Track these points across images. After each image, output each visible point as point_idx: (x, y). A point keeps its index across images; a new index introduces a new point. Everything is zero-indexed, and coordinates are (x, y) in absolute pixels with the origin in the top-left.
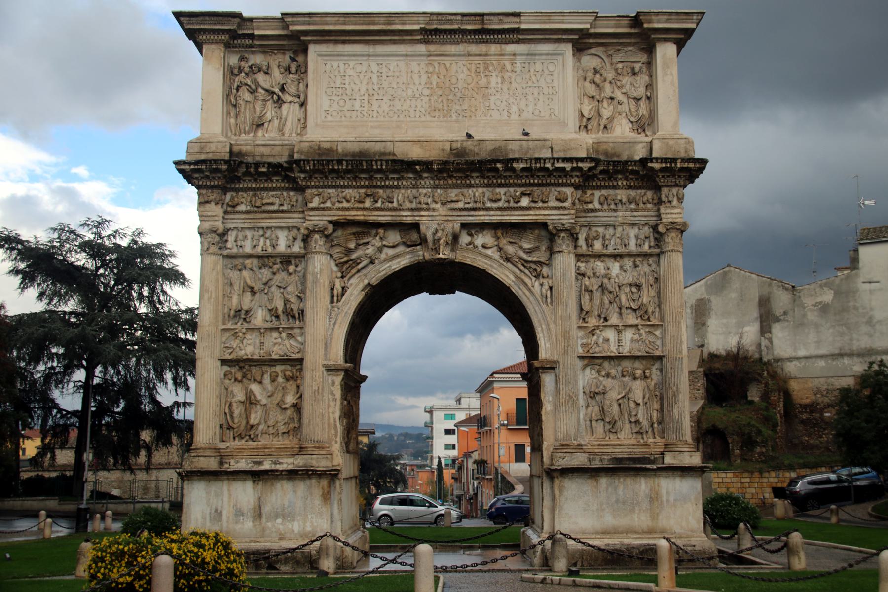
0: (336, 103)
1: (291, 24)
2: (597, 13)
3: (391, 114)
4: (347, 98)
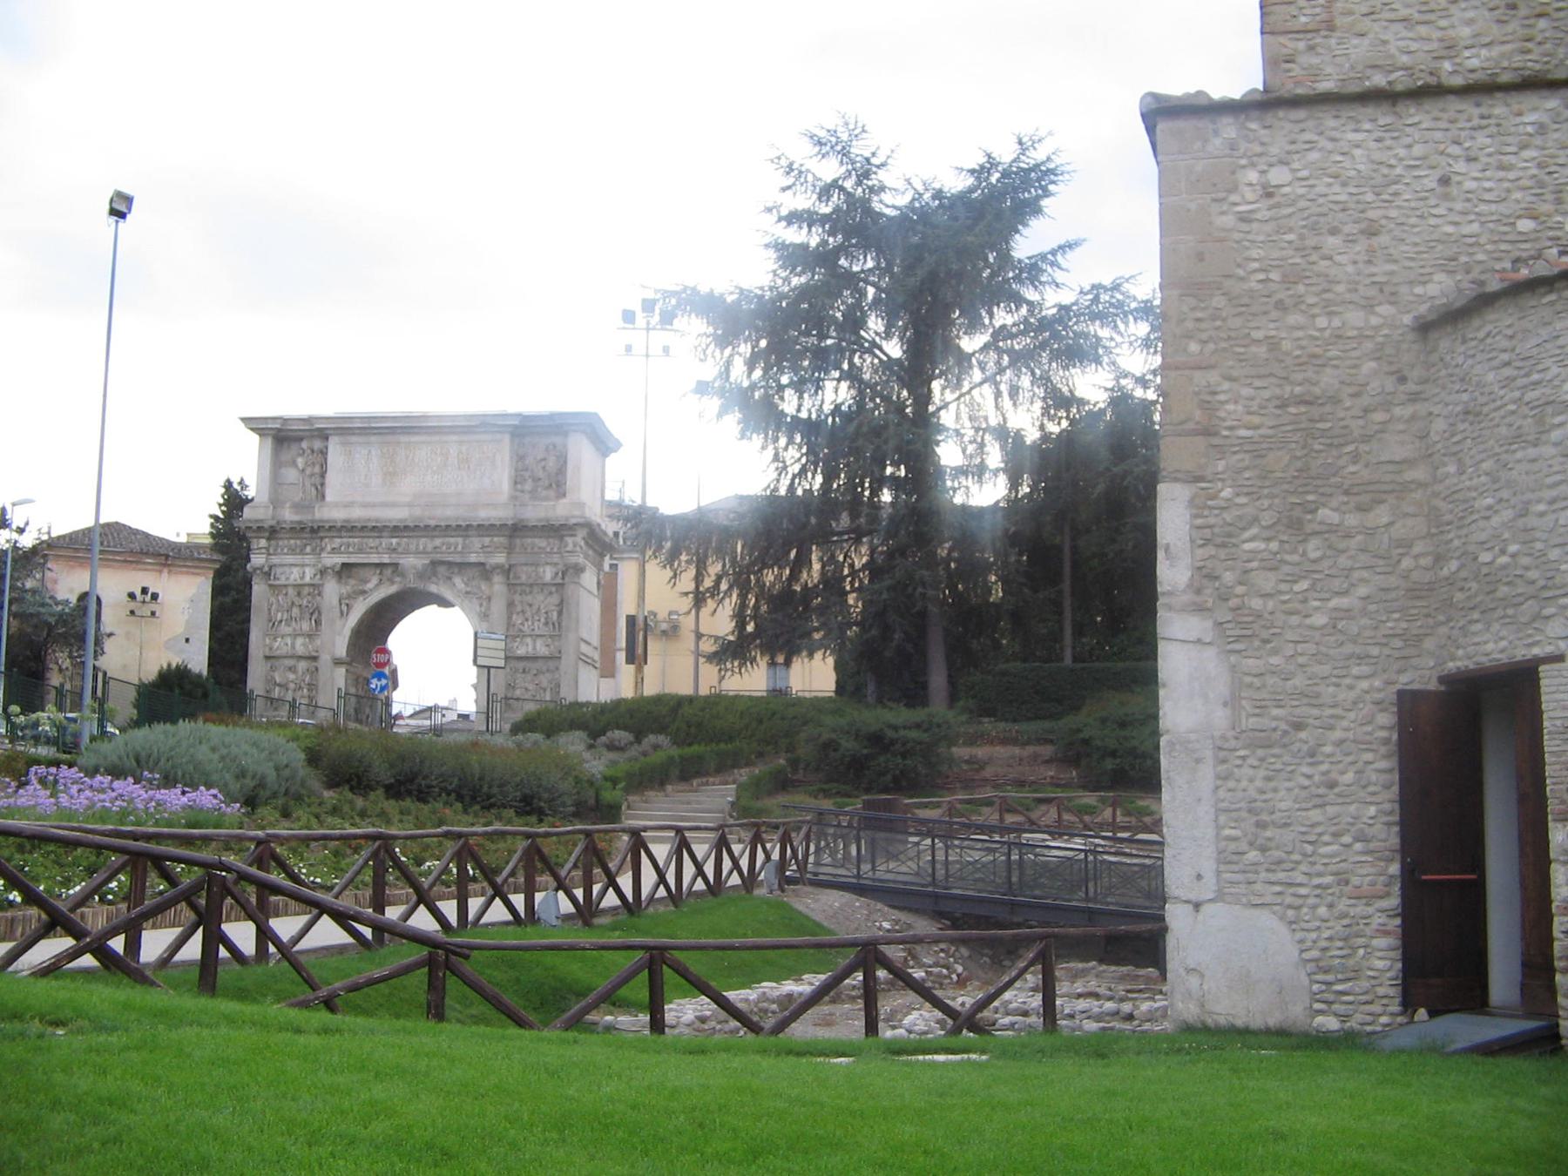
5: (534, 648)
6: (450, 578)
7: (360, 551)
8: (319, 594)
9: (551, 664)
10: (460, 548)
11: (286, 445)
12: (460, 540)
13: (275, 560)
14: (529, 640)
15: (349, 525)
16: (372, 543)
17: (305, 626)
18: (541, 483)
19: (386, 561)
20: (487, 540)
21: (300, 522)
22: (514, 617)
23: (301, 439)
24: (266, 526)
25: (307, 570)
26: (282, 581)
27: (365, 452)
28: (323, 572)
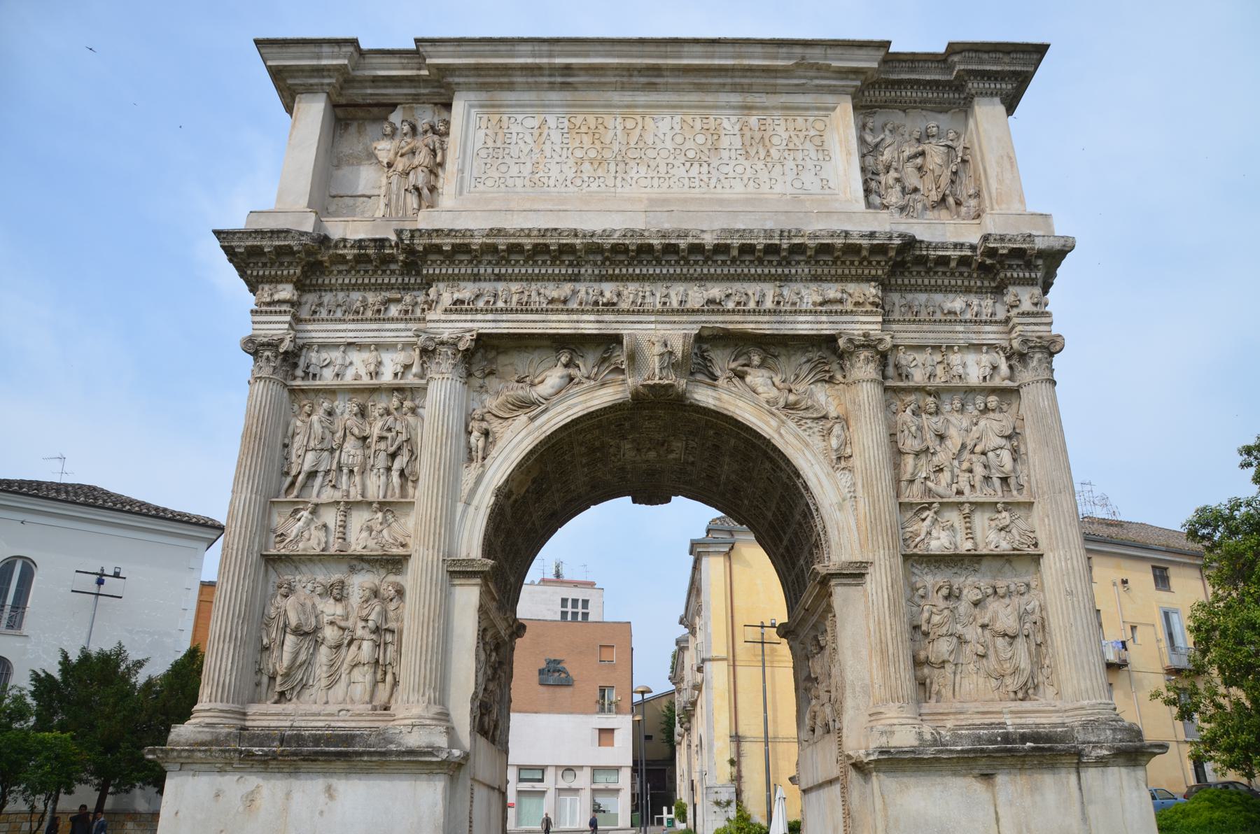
0: (494, 168)
1: (430, 57)
2: (887, 44)
3: (578, 182)
5: (970, 536)
6: (741, 376)
7: (524, 308)
8: (413, 411)
10: (769, 304)
11: (353, 129)
14: (954, 517)
15: (502, 243)
16: (552, 291)
18: (917, 196)
20: (832, 291)
21: (381, 243)
22: (909, 461)
23: (393, 106)
26: (327, 378)
27: (535, 123)
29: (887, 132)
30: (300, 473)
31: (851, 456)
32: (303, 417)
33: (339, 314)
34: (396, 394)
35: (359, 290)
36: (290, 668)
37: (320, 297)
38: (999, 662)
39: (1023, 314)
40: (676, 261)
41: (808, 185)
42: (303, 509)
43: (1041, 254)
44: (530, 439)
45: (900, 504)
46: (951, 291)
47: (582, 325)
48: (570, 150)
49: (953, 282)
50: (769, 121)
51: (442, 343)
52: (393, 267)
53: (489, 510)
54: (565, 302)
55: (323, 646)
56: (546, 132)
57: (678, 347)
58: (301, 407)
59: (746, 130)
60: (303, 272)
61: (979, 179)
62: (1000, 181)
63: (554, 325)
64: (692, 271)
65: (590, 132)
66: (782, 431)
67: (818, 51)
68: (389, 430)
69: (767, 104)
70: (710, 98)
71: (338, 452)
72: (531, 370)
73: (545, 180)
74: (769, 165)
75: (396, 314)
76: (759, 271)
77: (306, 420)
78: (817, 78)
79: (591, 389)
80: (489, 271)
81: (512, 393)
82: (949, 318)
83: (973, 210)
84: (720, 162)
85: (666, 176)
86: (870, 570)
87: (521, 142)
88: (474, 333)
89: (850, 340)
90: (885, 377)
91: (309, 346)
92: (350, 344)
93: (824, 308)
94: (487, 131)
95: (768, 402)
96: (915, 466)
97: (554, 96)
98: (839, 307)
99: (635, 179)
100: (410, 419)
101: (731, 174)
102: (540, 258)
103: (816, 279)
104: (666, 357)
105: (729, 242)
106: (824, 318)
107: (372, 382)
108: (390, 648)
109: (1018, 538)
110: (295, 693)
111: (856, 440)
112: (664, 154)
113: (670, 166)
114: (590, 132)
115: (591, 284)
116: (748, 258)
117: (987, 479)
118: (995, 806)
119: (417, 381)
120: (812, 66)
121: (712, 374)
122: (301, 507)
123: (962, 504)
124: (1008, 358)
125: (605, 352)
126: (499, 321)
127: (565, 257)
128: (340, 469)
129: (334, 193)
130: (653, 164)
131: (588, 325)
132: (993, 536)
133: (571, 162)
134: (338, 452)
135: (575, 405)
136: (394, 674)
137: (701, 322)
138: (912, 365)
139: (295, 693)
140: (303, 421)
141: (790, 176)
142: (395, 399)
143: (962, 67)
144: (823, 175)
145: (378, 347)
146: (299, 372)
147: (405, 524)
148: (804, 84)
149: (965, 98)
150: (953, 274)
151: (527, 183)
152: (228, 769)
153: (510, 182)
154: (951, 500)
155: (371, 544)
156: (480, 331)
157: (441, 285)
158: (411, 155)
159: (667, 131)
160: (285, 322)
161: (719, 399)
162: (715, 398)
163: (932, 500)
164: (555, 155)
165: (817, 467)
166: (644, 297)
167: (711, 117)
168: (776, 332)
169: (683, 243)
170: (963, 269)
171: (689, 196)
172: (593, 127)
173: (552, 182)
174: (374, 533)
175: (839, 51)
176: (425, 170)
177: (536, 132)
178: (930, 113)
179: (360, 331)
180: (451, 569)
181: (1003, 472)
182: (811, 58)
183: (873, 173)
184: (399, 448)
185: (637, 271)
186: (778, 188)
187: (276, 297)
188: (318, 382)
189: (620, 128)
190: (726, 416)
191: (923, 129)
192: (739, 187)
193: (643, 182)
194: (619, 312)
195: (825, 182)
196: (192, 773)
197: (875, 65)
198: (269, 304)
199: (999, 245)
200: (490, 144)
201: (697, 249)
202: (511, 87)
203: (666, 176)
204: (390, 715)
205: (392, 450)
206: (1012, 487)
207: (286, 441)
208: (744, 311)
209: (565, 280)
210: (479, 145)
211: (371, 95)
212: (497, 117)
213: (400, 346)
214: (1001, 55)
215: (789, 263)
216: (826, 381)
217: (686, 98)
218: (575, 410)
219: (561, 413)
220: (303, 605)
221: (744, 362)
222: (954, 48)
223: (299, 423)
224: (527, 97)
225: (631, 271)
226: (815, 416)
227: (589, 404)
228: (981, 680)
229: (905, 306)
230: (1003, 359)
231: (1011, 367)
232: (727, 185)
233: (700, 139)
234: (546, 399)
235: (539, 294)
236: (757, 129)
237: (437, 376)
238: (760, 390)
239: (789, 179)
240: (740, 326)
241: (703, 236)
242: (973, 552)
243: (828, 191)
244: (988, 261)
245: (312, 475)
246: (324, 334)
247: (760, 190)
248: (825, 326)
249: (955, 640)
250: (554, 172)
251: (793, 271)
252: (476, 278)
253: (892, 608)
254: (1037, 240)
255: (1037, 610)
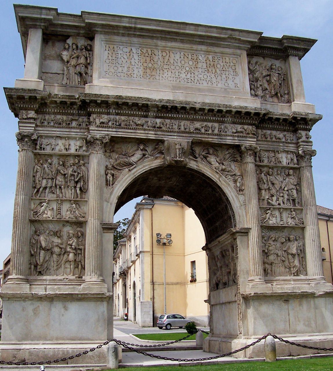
0: (112, 68)
4: (119, 66)
6: (206, 157)
7: (128, 127)
9: (298, 233)
10: (216, 131)
11: (50, 44)
12: (216, 125)
13: (42, 131)
15: (120, 101)
17: (69, 194)
19: (152, 137)
20: (239, 127)
22: (263, 192)
23: (68, 37)
24: (38, 97)
25: (72, 142)
26: (48, 151)
27: (128, 50)
28: (90, 143)
29: (257, 66)
30: (40, 188)
31: (244, 190)
32: (40, 165)
33: (52, 124)
34: (77, 157)
35: (60, 115)
36: (43, 263)
37: (45, 116)
38: (289, 263)
39: (303, 142)
40: (184, 113)
41: (230, 85)
42: (43, 202)
43: (311, 120)
44: (130, 178)
45: (260, 207)
46: (279, 130)
47: (149, 135)
48: (142, 63)
49: (280, 127)
50: (216, 58)
51: (97, 139)
52: (75, 107)
53: (115, 205)
54: (143, 126)
55: (54, 255)
56: (132, 54)
57: (185, 145)
58: (39, 161)
59: (208, 61)
60: (39, 107)
61: (289, 87)
62: (297, 90)
63: (139, 135)
64: (190, 117)
65: (149, 56)
66: (220, 179)
67: (237, 33)
68: (75, 172)
69: (216, 51)
70: (195, 47)
71: (55, 180)
72: (128, 151)
73: (132, 74)
74: (216, 76)
75: (75, 126)
76: (214, 118)
77: (41, 166)
78: (235, 43)
79: (152, 160)
80: (114, 111)
81: (122, 160)
82: (278, 140)
83: (286, 99)
84: (198, 73)
85: (178, 77)
86: (251, 231)
87: (122, 58)
88: (110, 136)
89: (245, 147)
90: (256, 161)
91: (41, 137)
92: (57, 136)
93: (236, 135)
94: (108, 52)
95: (215, 168)
96: (265, 194)
97: (135, 40)
98: (241, 134)
99: (166, 77)
100: (83, 168)
101: (202, 78)
102: (134, 108)
103: (234, 123)
104: (181, 150)
105: (204, 107)
106: (236, 138)
107: (67, 152)
108: (80, 255)
109: (297, 221)
110: (44, 272)
111: (246, 184)
112: (177, 68)
113: (180, 73)
114: (149, 56)
115: (153, 119)
116: (211, 113)
117: (288, 200)
118: (288, 310)
119: (85, 153)
120: (234, 38)
121: (196, 156)
122: (43, 201)
123: (280, 208)
124: (297, 157)
125: (156, 145)
126: (118, 132)
127: (143, 108)
128: (56, 186)
129: (44, 71)
130: (173, 71)
131: (152, 136)
132: (290, 221)
133: (142, 68)
134: (55, 180)
135: (146, 166)
136: (81, 265)
137: (193, 137)
138: (264, 157)
139: (44, 272)
140: (40, 167)
141: (224, 81)
142: (76, 160)
143: (287, 45)
144: (235, 81)
145: (69, 138)
146: (38, 147)
147: (84, 208)
148: (230, 45)
149: (286, 56)
150: (280, 124)
151: (126, 75)
152: (27, 300)
153: (119, 75)
154: (276, 207)
155: (72, 216)
156: (112, 135)
157: (95, 116)
158: (76, 58)
159: (179, 59)
160: (33, 127)
161: (198, 166)
162: (197, 166)
163: (271, 207)
164: (136, 65)
165: (232, 193)
166: (172, 126)
167: (195, 54)
168: (219, 142)
169: (188, 107)
170: (284, 123)
171: (187, 86)
172: (150, 54)
173: (135, 76)
174: (72, 212)
175: (244, 34)
176: (84, 66)
177: (128, 54)
178: (273, 59)
179: (62, 131)
180: (103, 227)
181: (293, 197)
182: (234, 35)
183: (252, 81)
184: (79, 179)
185: (170, 115)
186: (220, 85)
187: (29, 116)
188: (45, 151)
189: (160, 55)
190: (201, 173)
191: (270, 64)
192: (205, 84)
193: (170, 79)
194: (163, 131)
195: (236, 84)
196: (12, 301)
197: (257, 40)
198: (26, 119)
199: (297, 116)
200: (110, 58)
201: (193, 109)
202: (118, 34)
203: (178, 77)
204: (83, 280)
205: (76, 180)
206: (296, 203)
207: (34, 175)
208: (208, 134)
209: (142, 117)
210: (106, 57)
211: (60, 31)
212: (111, 46)
213: (78, 139)
214: (300, 42)
215: (225, 117)
216: (235, 161)
217: (186, 46)
218: (146, 167)
219: (141, 168)
220: (46, 239)
221: (207, 152)
222: (285, 38)
223: (39, 168)
224: (124, 39)
225: (167, 115)
226: (231, 174)
227: (151, 166)
228: (283, 269)
229: (263, 135)
230: (295, 157)
231: (297, 160)
232: (201, 83)
233: (191, 63)
234: (135, 163)
235: (133, 122)
236: (212, 61)
237: (95, 152)
238: (213, 163)
239: (223, 83)
240: (207, 139)
241: (196, 104)
242: (283, 226)
243: (237, 88)
244: (293, 121)
245: (45, 188)
246: (47, 132)
247: (213, 86)
248: (236, 141)
249: (276, 255)
250: (136, 72)
251: (226, 120)
252: (108, 114)
253: (258, 244)
254: (310, 115)
255: (302, 246)
